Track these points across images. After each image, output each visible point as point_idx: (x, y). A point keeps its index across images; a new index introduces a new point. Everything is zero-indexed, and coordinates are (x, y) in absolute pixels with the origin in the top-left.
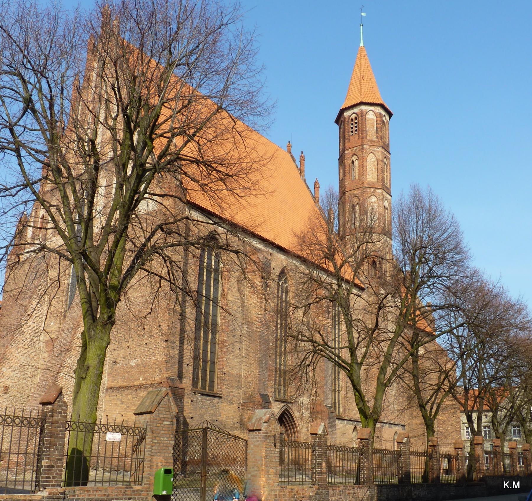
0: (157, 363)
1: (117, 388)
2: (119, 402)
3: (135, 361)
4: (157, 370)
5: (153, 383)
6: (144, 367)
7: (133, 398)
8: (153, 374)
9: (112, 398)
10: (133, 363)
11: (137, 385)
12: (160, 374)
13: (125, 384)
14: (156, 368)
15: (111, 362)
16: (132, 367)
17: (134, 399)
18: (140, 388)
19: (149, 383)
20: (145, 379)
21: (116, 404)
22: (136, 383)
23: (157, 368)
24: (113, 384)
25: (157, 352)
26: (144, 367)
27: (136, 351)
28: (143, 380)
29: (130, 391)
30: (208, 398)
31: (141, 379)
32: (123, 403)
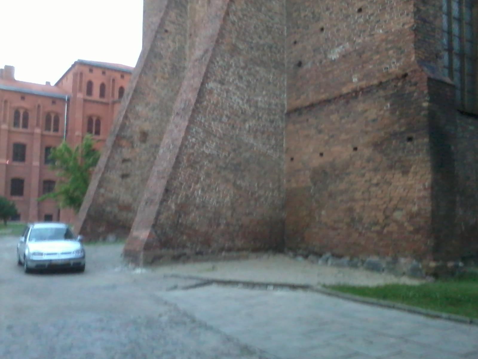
0: (391, 38)
1: (306, 107)
2: (313, 132)
3: (338, 50)
4: (391, 52)
5: (384, 80)
6: (360, 55)
7: (342, 118)
8: (381, 63)
9: (298, 126)
10: (334, 55)
11: (348, 94)
12: (398, 60)
13: (323, 97)
14: (387, 50)
15: (292, 66)
16: (333, 62)
17: (343, 121)
18: (356, 97)
19: (375, 82)
20: (367, 76)
21: (307, 136)
22: (345, 90)
23: (391, 48)
24: (298, 103)
25: (387, 17)
26: (360, 55)
27: (338, 30)
28: (360, 80)
29: (333, 107)
30: (470, 120)
31: (355, 80)
32: (320, 132)
